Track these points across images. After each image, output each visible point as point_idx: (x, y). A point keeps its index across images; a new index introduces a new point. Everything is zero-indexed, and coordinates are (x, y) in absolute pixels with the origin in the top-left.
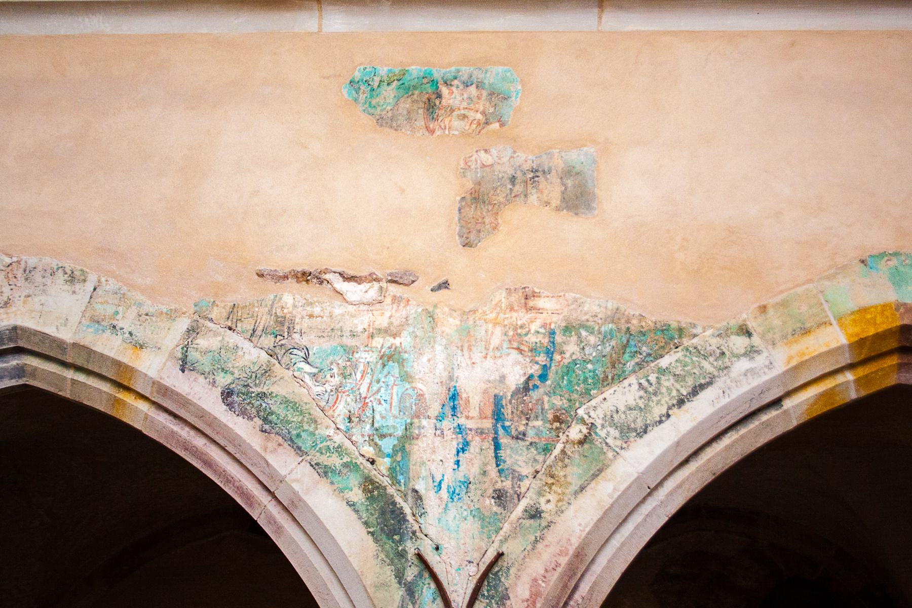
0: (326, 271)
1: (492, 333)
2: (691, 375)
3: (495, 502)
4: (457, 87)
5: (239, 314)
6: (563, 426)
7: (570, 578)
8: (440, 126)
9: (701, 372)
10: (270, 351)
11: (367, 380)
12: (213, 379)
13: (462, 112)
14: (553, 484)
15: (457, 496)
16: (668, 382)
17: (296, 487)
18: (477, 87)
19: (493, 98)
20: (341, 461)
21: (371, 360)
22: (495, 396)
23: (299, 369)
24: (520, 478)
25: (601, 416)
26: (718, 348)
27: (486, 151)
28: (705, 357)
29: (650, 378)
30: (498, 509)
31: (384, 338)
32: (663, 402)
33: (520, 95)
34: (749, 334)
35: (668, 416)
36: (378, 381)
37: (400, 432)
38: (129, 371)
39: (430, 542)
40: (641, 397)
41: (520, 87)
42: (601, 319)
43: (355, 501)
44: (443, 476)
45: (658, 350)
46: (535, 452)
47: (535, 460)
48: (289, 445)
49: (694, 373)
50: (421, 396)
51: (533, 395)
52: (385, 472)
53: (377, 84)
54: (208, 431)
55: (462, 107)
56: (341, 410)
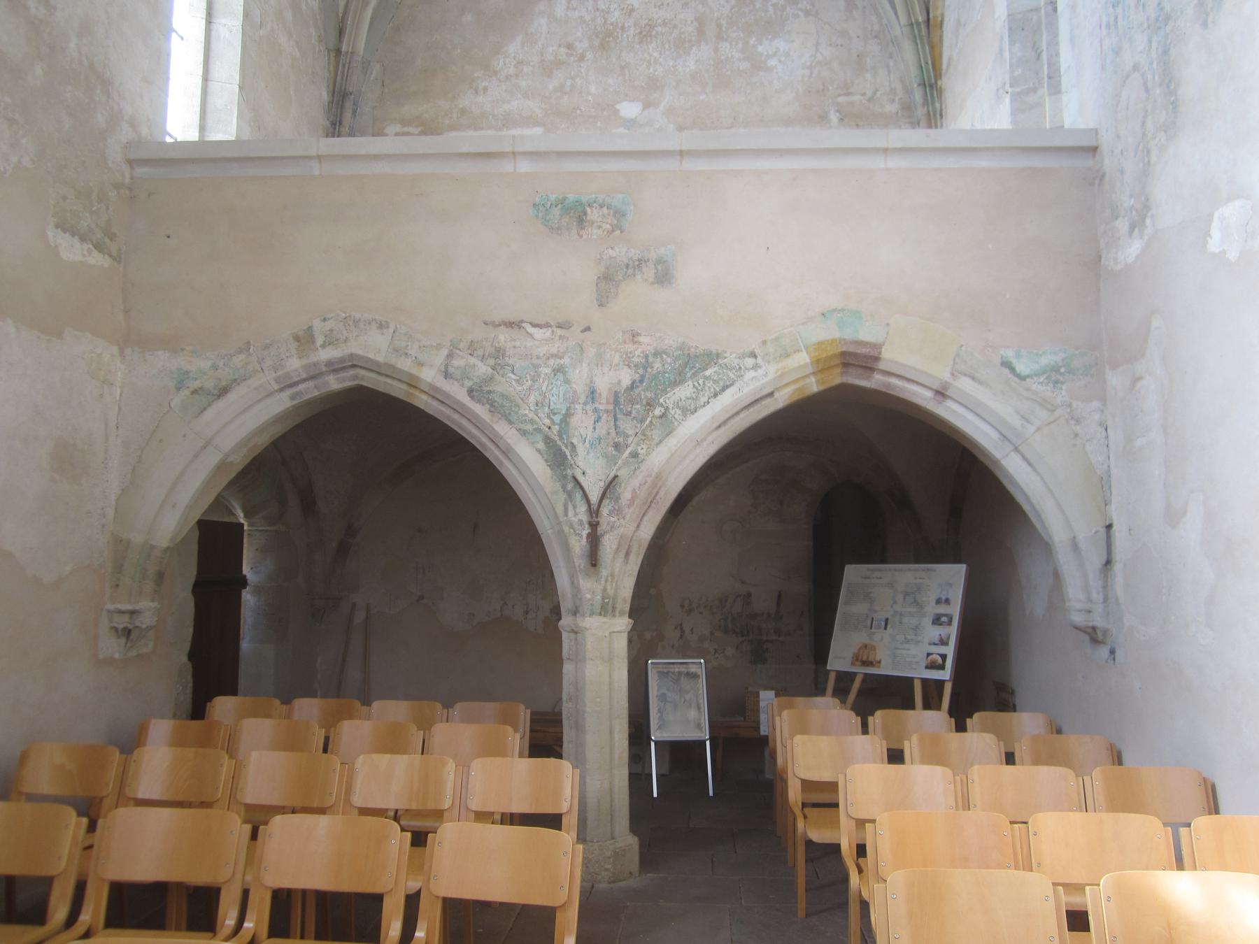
0: (522, 322)
1: (614, 357)
4: (596, 208)
11: (546, 383)
13: (599, 224)
16: (709, 384)
17: (509, 441)
18: (608, 208)
23: (509, 377)
25: (672, 402)
27: (612, 248)
32: (706, 395)
34: (756, 357)
35: (708, 402)
38: (418, 379)
40: (694, 392)
41: (632, 208)
47: (636, 427)
50: (575, 392)
52: (556, 433)
53: (549, 206)
54: (460, 411)
55: (599, 220)
56: (532, 399)
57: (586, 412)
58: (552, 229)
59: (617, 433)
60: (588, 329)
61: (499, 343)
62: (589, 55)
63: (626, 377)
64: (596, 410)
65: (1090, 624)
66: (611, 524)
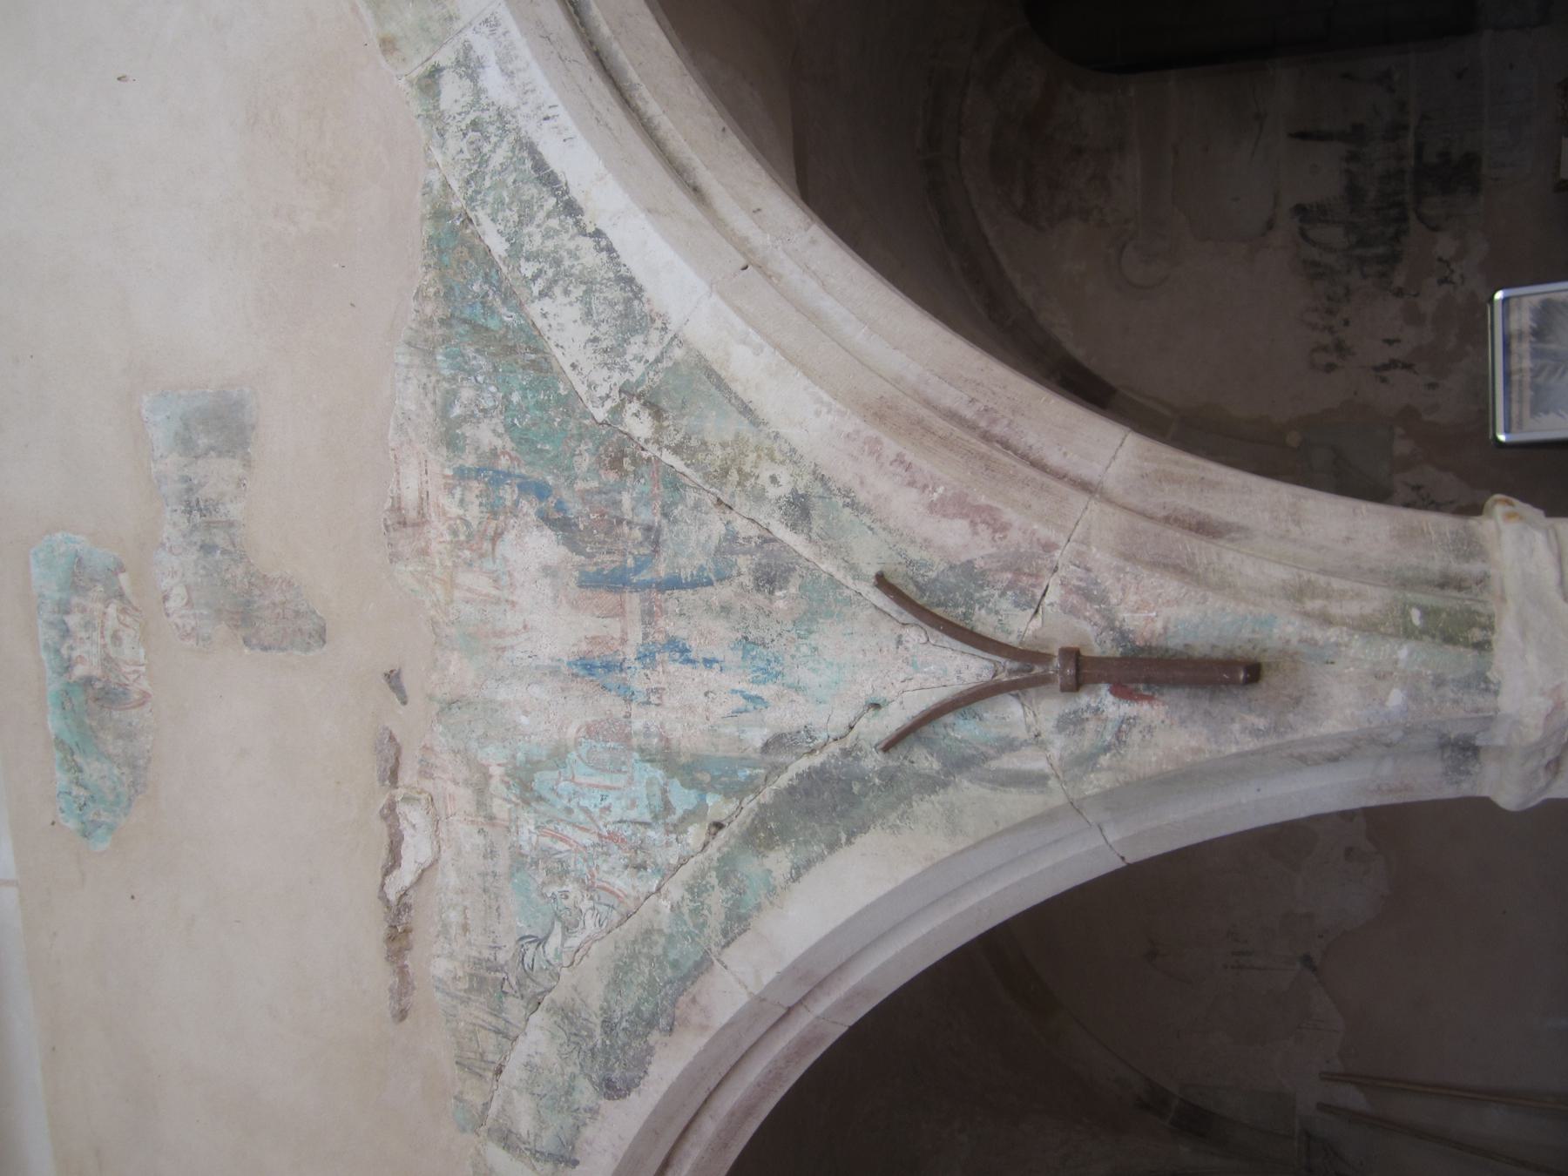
1: (469, 590)
2: (518, 189)
3: (781, 589)
4: (71, 648)
5: (472, 1055)
6: (628, 450)
7: (928, 430)
8: (135, 681)
9: (512, 167)
10: (530, 1006)
11: (568, 831)
12: (585, 1111)
13: (108, 640)
14: (740, 471)
15: (773, 664)
16: (534, 239)
17: (768, 976)
18: (67, 613)
19: (82, 584)
20: (717, 888)
21: (532, 821)
22: (580, 586)
23: (558, 956)
24: (731, 537)
25: (605, 372)
26: (465, 135)
27: (166, 598)
28: (484, 161)
29: (529, 275)
31: (492, 796)
32: (571, 245)
33: (71, 535)
34: (435, 72)
35: (598, 234)
36: (569, 811)
37: (659, 774)
39: (863, 721)
40: (566, 292)
41: (59, 536)
42: (429, 376)
43: (789, 864)
44: (734, 691)
45: (476, 260)
46: (680, 507)
47: (696, 506)
48: (693, 984)
49: (514, 182)
50: (591, 731)
51: (574, 511)
52: (732, 806)
53: (82, 792)
54: (683, 1120)
55: (100, 641)
56: (622, 882)
57: (655, 691)
58: (134, 784)
59: (721, 579)
60: (393, 680)
61: (455, 978)
66: (1074, 599)
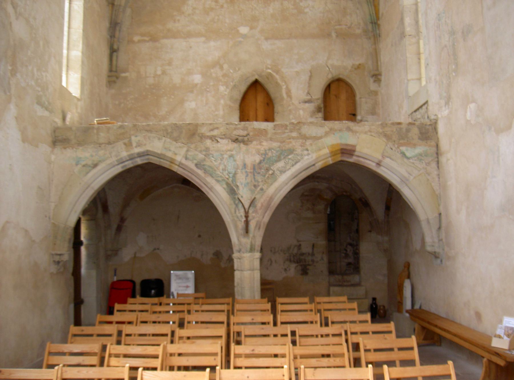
17: (212, 184)
28: (298, 155)
30: (255, 189)
37: (233, 173)
38: (174, 160)
50: (238, 165)
54: (191, 172)
56: (221, 167)
62: (225, 6)
63: (257, 159)
64: (246, 172)
65: (433, 251)
